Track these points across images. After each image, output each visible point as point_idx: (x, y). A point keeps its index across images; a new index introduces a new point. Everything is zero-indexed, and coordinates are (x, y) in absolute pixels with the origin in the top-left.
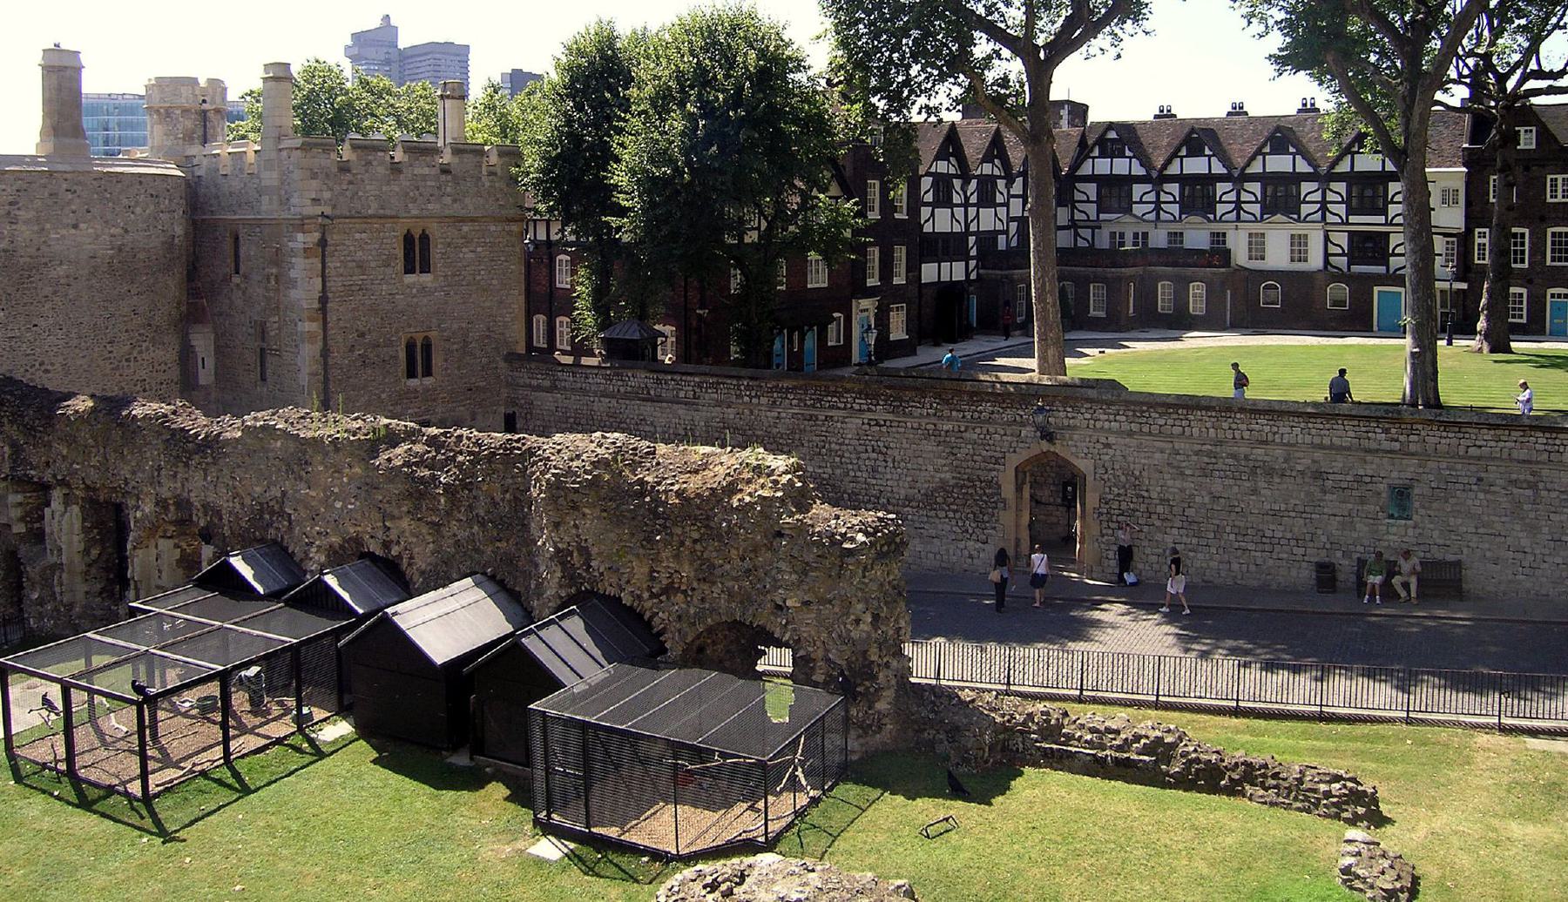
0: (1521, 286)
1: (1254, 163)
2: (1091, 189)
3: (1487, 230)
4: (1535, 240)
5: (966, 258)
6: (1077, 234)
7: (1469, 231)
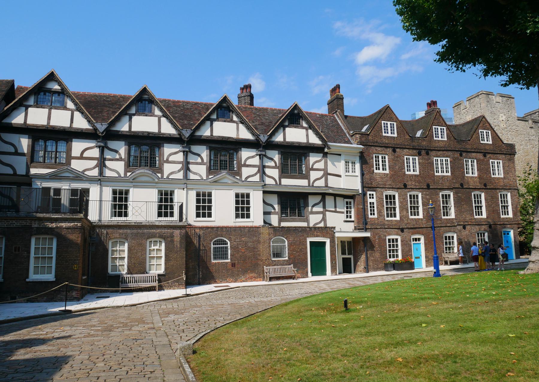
0: (397, 234)
1: (203, 128)
3: (374, 193)
4: (402, 200)
7: (364, 194)
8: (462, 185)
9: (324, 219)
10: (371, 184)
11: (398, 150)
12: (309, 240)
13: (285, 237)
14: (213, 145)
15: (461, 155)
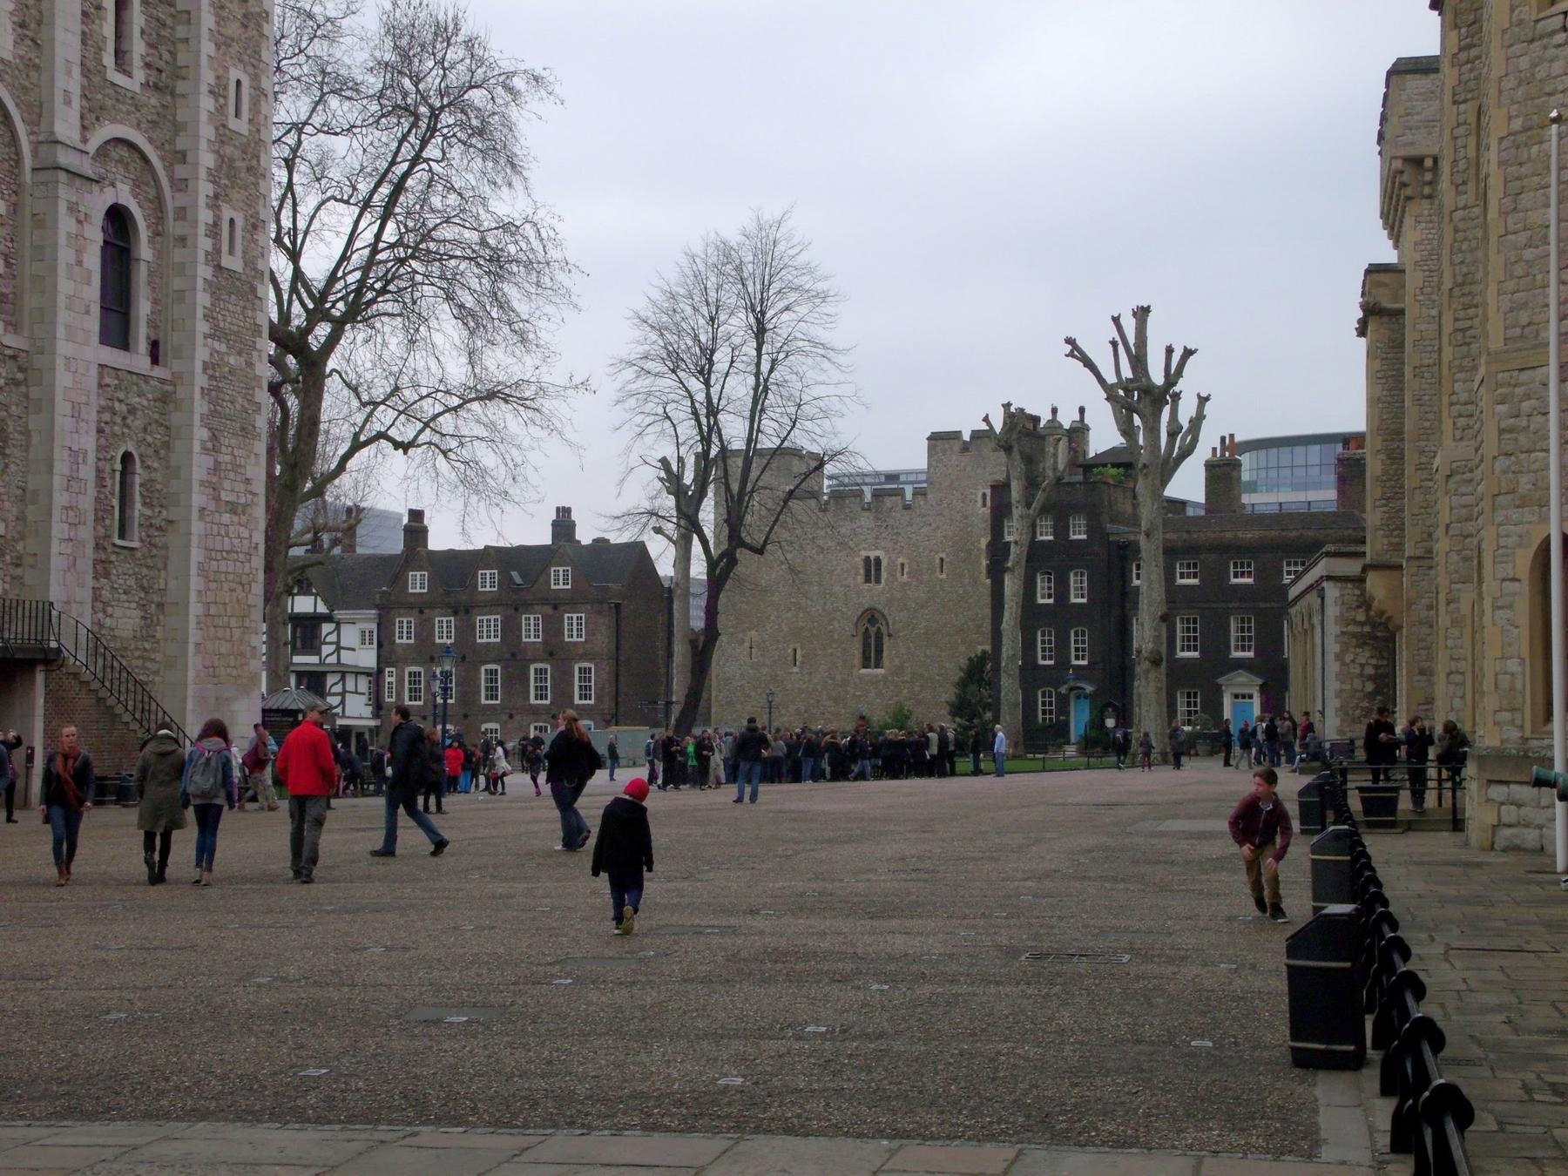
7: (380, 671)
8: (513, 655)
9: (343, 702)
11: (426, 611)
15: (516, 609)
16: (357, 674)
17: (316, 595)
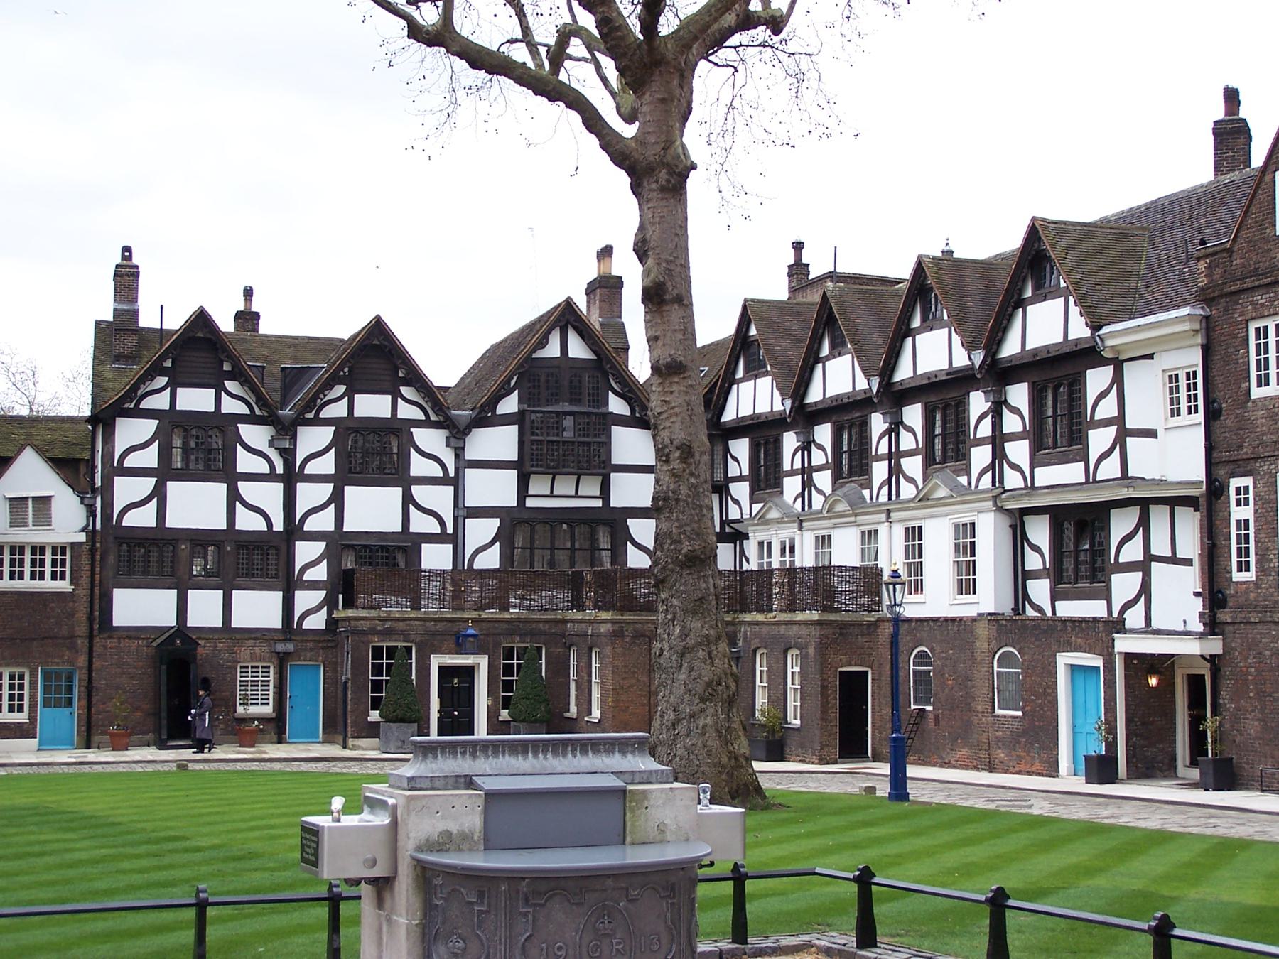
2: (741, 448)
3: (1247, 481)
5: (289, 584)
6: (742, 553)
9: (1145, 589)
10: (1240, 447)
12: (1064, 660)
13: (1018, 647)
14: (932, 398)
16: (1173, 502)
17: (1066, 294)
